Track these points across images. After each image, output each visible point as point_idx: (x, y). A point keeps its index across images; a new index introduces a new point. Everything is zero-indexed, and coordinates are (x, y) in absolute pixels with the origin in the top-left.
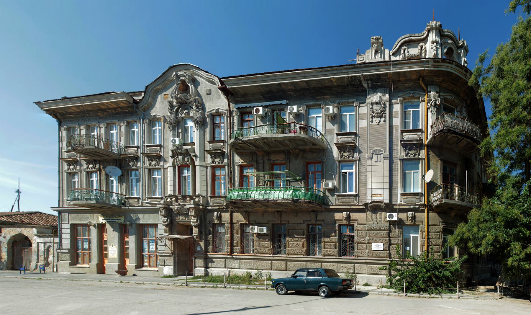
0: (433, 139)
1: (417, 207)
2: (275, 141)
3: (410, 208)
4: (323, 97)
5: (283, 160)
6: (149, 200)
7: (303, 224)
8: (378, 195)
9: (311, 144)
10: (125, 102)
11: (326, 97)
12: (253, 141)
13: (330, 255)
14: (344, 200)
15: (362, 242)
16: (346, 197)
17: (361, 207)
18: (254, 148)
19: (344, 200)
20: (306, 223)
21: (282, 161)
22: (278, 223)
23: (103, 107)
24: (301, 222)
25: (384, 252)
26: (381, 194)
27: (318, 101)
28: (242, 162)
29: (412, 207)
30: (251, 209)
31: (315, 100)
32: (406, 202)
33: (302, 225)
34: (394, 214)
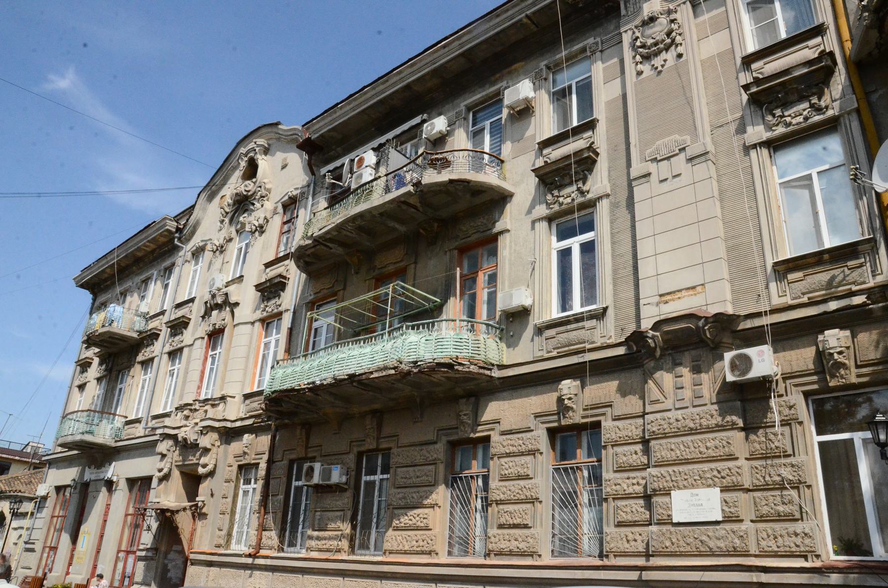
0: (874, 34)
1: (858, 300)
2: (381, 214)
3: (825, 313)
4: (507, 70)
5: (401, 261)
6: (154, 422)
7: (435, 443)
8: (684, 293)
9: (468, 196)
10: (166, 233)
11: (513, 67)
12: (335, 233)
13: (511, 554)
14: (563, 338)
15: (630, 490)
16: (569, 327)
17: (621, 351)
18: (340, 250)
19: (563, 338)
20: (444, 439)
21: (398, 265)
22: (371, 447)
23: (140, 254)
24: (430, 437)
25: (728, 526)
26: (693, 288)
27: (494, 86)
28: (315, 294)
29: (833, 306)
30: (316, 416)
31: (487, 86)
32: (804, 294)
33: (431, 447)
34: (751, 352)
